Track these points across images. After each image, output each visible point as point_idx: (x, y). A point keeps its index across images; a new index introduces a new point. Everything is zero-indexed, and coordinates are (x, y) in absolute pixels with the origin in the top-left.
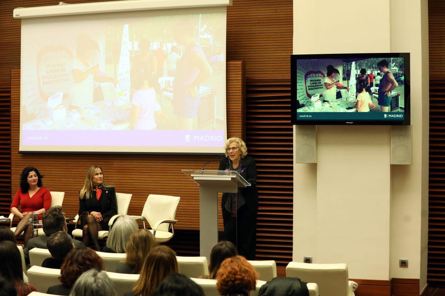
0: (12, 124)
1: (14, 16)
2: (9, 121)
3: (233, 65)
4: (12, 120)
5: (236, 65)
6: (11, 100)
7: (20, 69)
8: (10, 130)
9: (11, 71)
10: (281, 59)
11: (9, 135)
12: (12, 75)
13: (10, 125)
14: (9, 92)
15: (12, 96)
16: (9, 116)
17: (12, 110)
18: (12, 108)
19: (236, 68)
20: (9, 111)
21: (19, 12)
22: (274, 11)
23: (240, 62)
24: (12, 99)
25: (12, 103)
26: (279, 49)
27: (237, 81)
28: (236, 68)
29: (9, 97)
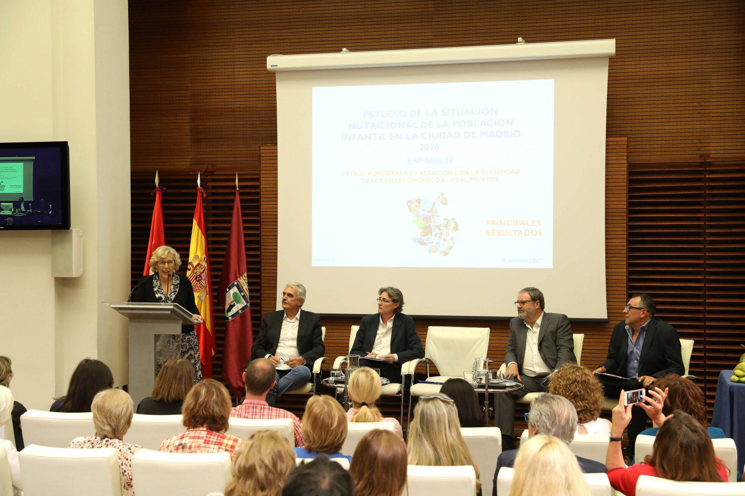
0: (262, 227)
1: (269, 67)
2: (258, 222)
3: (615, 143)
4: (262, 220)
5: (620, 143)
7: (277, 146)
8: (259, 235)
9: (260, 150)
11: (259, 242)
12: (261, 155)
13: (258, 228)
14: (258, 180)
15: (262, 186)
16: (258, 215)
17: (262, 207)
19: (618, 147)
21: (274, 61)
22: (665, 65)
23: (625, 139)
25: (262, 196)
27: (620, 165)
29: (258, 187)
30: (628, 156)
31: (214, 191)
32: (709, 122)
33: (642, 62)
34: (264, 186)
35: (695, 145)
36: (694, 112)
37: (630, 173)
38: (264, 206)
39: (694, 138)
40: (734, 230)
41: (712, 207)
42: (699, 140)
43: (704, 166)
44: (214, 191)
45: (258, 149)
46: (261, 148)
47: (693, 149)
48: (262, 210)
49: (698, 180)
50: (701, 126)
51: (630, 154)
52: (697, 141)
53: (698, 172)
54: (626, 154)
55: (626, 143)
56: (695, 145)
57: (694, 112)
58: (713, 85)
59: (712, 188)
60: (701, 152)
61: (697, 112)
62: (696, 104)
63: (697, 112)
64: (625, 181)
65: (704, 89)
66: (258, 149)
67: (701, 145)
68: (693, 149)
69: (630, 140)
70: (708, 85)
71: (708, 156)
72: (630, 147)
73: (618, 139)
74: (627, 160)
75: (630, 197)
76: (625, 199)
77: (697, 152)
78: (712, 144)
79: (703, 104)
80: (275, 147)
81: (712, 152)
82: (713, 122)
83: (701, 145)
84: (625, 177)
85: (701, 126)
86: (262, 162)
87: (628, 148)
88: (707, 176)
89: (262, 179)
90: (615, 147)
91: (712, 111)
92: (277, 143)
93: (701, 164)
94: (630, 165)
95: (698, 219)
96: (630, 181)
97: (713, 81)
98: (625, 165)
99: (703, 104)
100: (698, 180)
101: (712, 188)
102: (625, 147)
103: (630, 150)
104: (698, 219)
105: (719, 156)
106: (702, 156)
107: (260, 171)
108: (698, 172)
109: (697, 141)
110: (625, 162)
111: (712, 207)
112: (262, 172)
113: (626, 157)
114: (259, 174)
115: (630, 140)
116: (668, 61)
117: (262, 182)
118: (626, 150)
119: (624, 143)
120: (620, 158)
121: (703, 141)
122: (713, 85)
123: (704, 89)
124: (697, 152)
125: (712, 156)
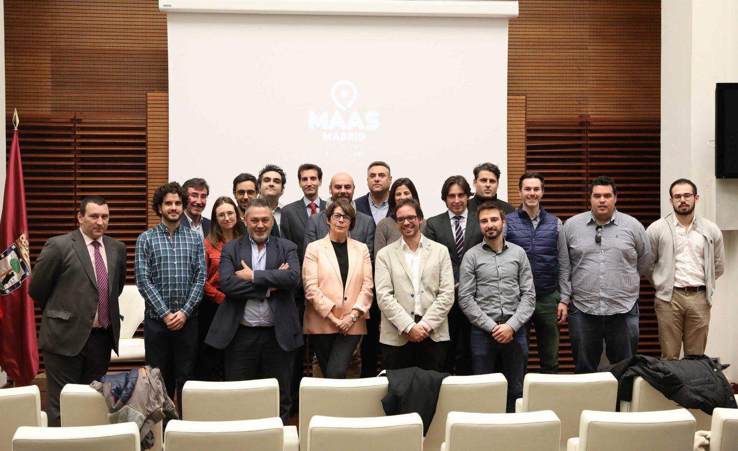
2: (145, 175)
3: (514, 101)
4: (149, 173)
5: (518, 101)
6: (147, 141)
7: (168, 93)
9: (147, 96)
10: (558, 96)
12: (149, 102)
14: (144, 129)
15: (149, 136)
16: (144, 168)
18: (149, 154)
19: (517, 105)
20: (144, 160)
23: (524, 97)
24: (149, 140)
26: (555, 82)
27: (519, 123)
28: (517, 105)
29: (144, 137)
30: (526, 114)
31: (581, 135)
32: (587, 85)
33: (528, 26)
34: (152, 135)
36: (574, 75)
37: (528, 131)
38: (152, 159)
39: (574, 99)
40: (632, 185)
41: (593, 164)
42: (579, 101)
43: (584, 124)
44: (581, 135)
45: (145, 92)
46: (149, 94)
48: (149, 162)
49: (579, 138)
50: (581, 89)
51: (528, 113)
52: (577, 103)
53: (579, 131)
54: (525, 112)
55: (524, 102)
57: (574, 75)
58: (590, 51)
59: (592, 146)
60: (581, 113)
61: (576, 75)
62: (576, 68)
63: (576, 75)
64: (524, 137)
65: (583, 54)
66: (144, 96)
67: (581, 106)
68: (574, 109)
69: (528, 99)
70: (585, 51)
72: (528, 106)
73: (517, 97)
74: (526, 117)
75: (528, 154)
76: (524, 155)
77: (577, 113)
79: (581, 68)
80: (165, 94)
81: (589, 113)
82: (590, 86)
83: (579, 106)
84: (524, 134)
85: (581, 89)
86: (149, 110)
87: (526, 106)
88: (589, 135)
89: (149, 128)
90: (515, 105)
91: (590, 75)
92: (168, 90)
93: (581, 124)
94: (528, 124)
95: (580, 175)
96: (529, 139)
97: (590, 47)
98: (524, 123)
99: (581, 68)
100: (579, 138)
101: (592, 146)
102: (524, 105)
103: (528, 109)
104: (580, 175)
105: (599, 117)
106: (581, 116)
107: (146, 120)
108: (579, 131)
109: (577, 103)
110: (524, 119)
111: (593, 164)
112: (148, 121)
113: (524, 116)
114: (146, 123)
115: (528, 99)
116: (550, 26)
117: (149, 132)
119: (523, 101)
120: (519, 115)
121: (582, 102)
122: (590, 51)
123: (583, 54)
124: (577, 113)
125: (591, 117)
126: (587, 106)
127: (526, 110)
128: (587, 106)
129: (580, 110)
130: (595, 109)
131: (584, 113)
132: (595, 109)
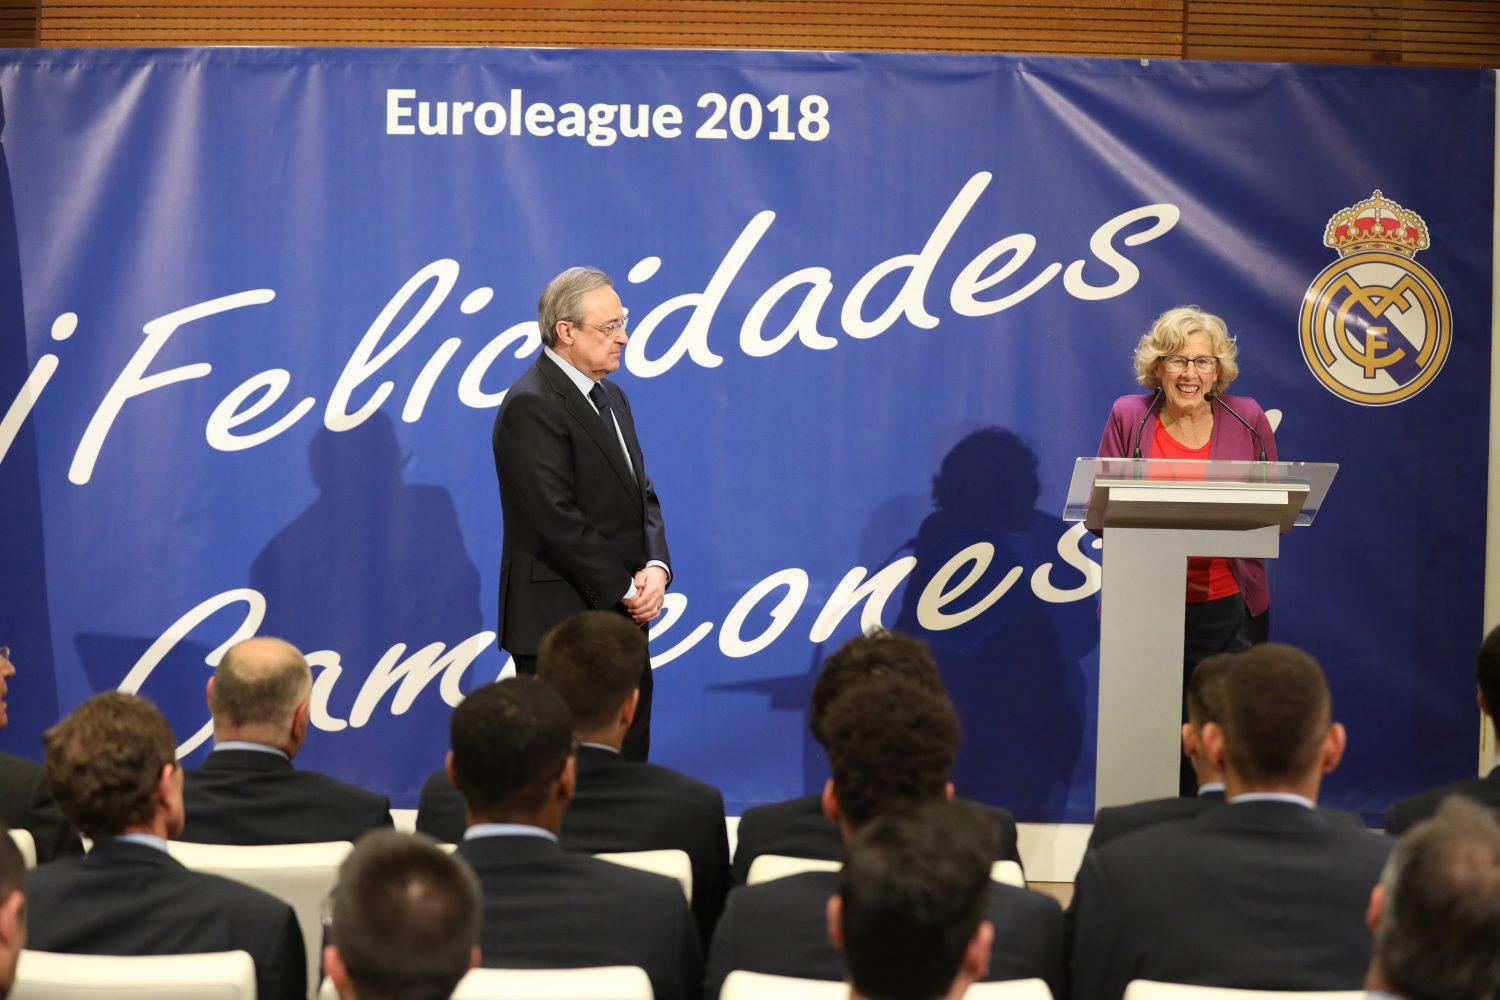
30: (1184, 44)
35: (1364, 24)
47: (1356, 34)
51: (1191, 39)
52: (1366, 13)
54: (1179, 38)
56: (1364, 24)
68: (1356, 34)
71: (1398, 55)
72: (1191, 18)
78: (1405, 25)
81: (1405, 46)
87: (1185, 22)
102: (1178, 17)
103: (1191, 29)
106: (1381, 55)
113: (1180, 47)
118: (1179, 27)
121: (1380, 12)
125: (1406, 57)
126: (1396, 25)
127: (1184, 33)
128: (1396, 25)
129: (1374, 35)
130: (1422, 36)
131: (1389, 46)
132: (1422, 36)
